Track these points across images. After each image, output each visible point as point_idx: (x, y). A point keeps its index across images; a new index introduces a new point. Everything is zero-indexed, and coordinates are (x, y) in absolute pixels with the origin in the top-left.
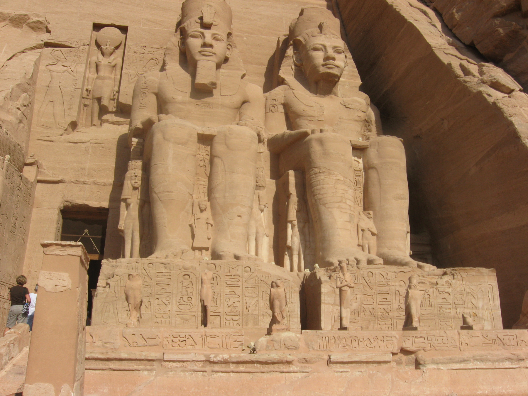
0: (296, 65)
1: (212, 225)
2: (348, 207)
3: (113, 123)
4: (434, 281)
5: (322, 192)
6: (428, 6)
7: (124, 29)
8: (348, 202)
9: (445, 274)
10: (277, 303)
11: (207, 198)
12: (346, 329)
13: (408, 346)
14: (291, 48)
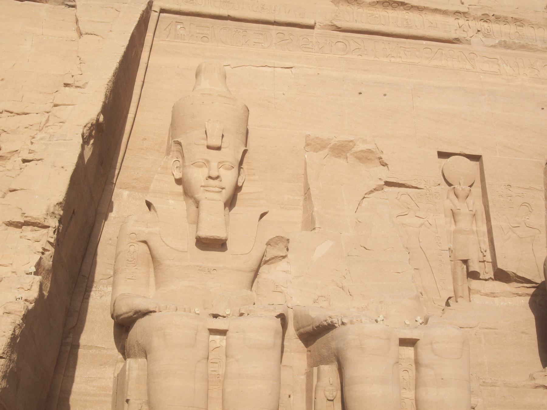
3: (486, 295)
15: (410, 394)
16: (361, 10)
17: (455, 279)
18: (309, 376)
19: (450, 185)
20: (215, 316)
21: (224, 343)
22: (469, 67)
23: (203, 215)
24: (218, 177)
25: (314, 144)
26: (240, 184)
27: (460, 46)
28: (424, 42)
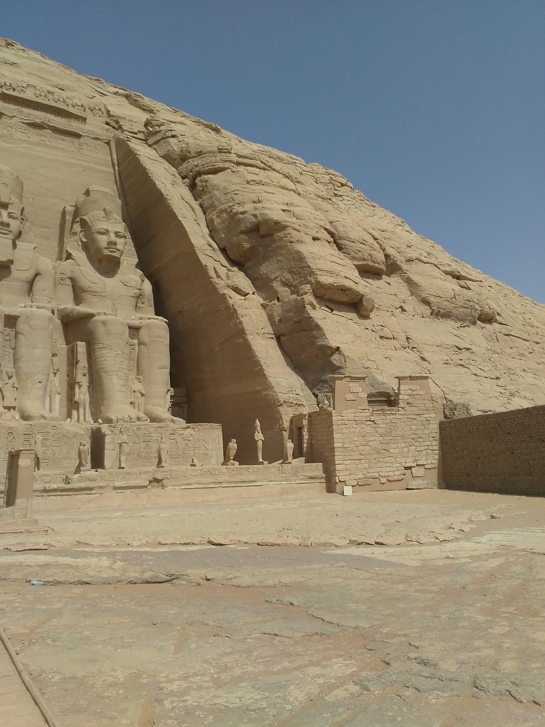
0: (82, 241)
1: (17, 389)
2: (124, 375)
4: (181, 432)
5: (105, 363)
6: (196, 200)
8: (125, 371)
9: (189, 427)
10: (83, 454)
11: (12, 366)
12: (123, 468)
13: (159, 476)
14: (78, 224)
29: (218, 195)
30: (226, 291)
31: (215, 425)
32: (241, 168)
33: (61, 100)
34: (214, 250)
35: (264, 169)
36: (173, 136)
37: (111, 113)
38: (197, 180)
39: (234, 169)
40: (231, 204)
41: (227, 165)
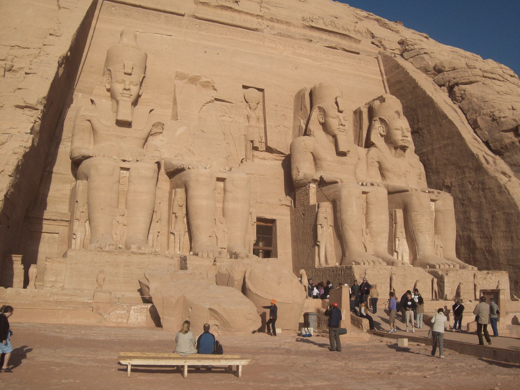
3: (261, 159)
6: (455, 104)
7: (262, 90)
9: (488, 273)
11: (365, 226)
15: (220, 205)
16: (209, 9)
17: (246, 150)
18: (170, 193)
19: (247, 102)
20: (124, 161)
21: (128, 175)
22: (261, 44)
23: (120, 108)
24: (129, 89)
25: (180, 76)
26: (140, 94)
27: (258, 33)
28: (240, 29)
29: (477, 102)
30: (497, 175)
31: (504, 272)
32: (488, 81)
33: (341, 27)
34: (479, 143)
35: (503, 81)
36: (425, 53)
37: (375, 35)
38: (454, 89)
39: (485, 82)
40: (492, 110)
41: (478, 79)
